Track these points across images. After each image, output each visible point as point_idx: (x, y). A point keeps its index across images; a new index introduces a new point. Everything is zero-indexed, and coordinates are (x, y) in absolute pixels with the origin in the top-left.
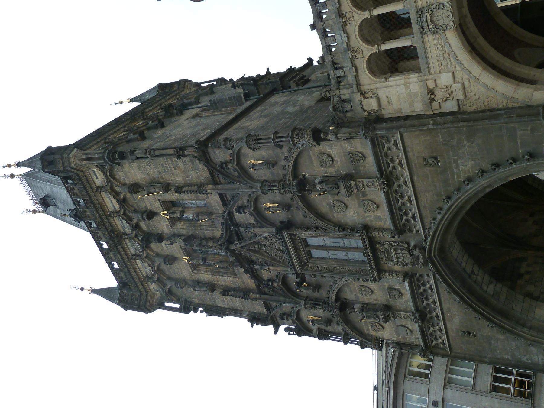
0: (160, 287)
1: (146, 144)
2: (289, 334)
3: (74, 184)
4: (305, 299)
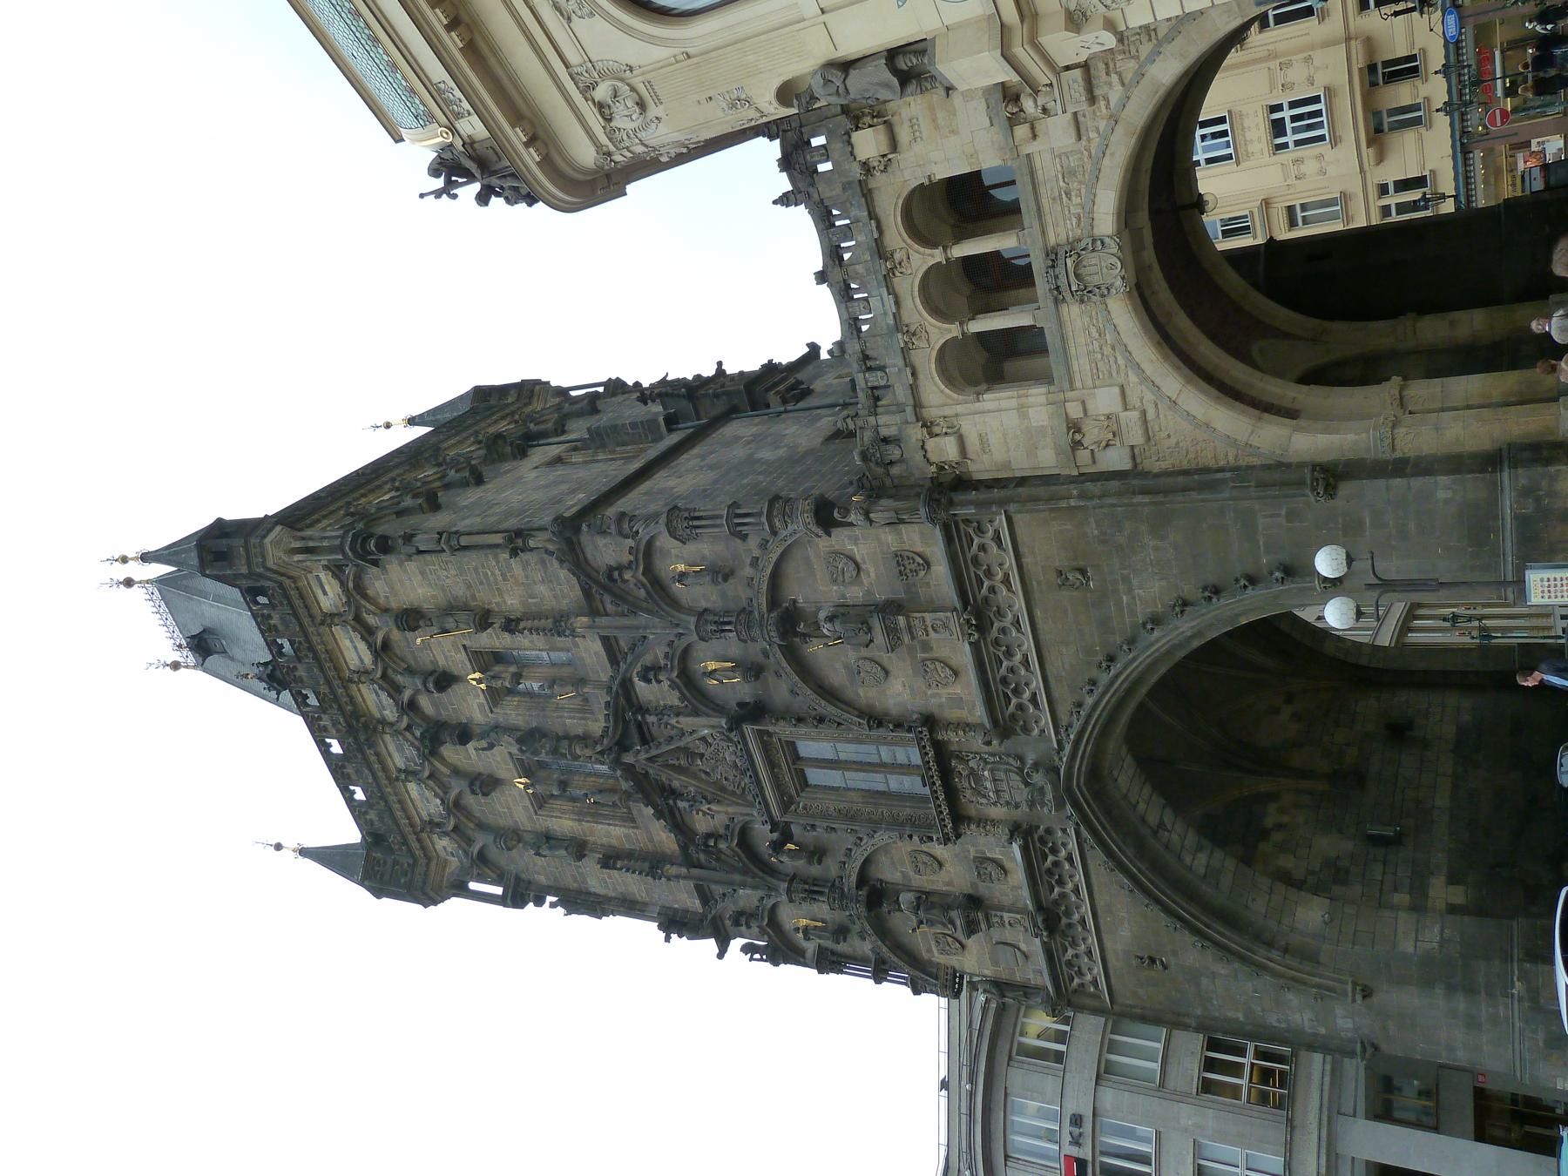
0: (460, 846)
1: (439, 520)
2: (751, 959)
3: (272, 606)
4: (788, 878)
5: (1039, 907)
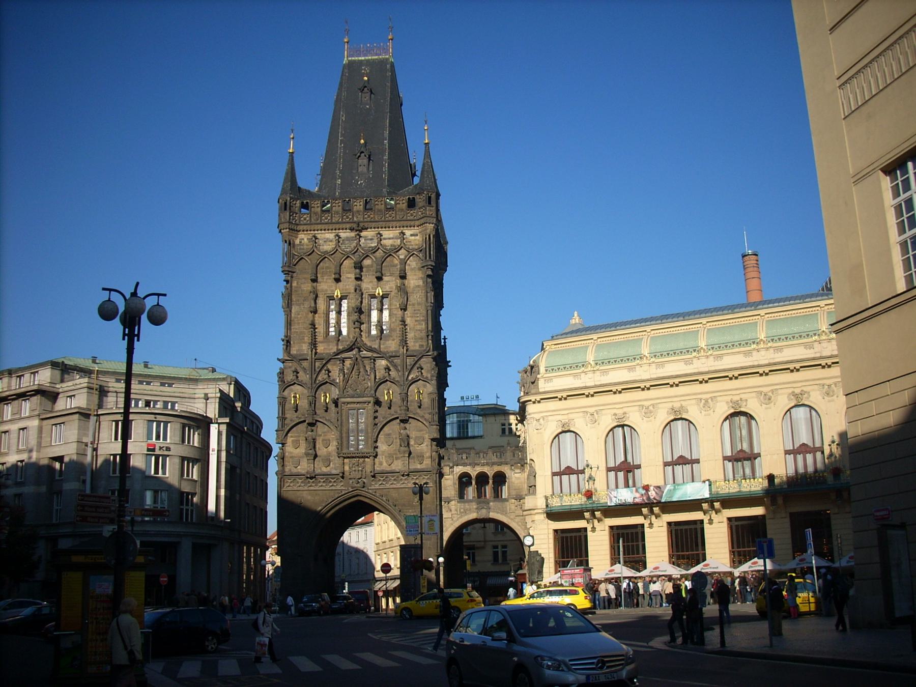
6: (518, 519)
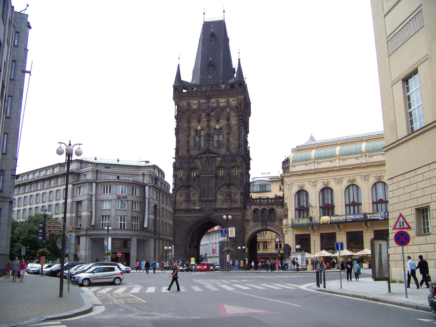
5: (190, 209)
6: (280, 230)
